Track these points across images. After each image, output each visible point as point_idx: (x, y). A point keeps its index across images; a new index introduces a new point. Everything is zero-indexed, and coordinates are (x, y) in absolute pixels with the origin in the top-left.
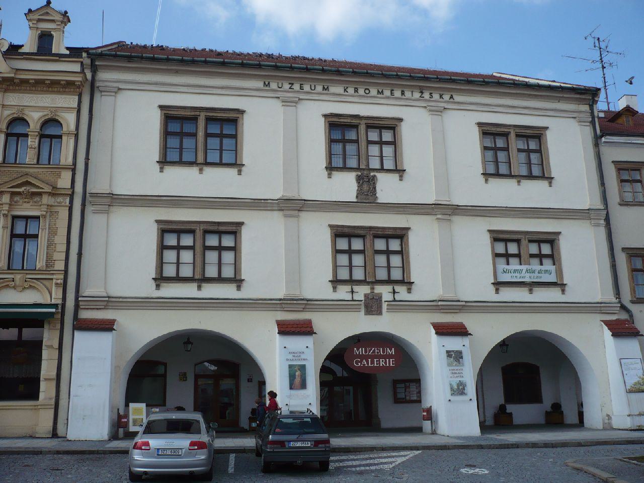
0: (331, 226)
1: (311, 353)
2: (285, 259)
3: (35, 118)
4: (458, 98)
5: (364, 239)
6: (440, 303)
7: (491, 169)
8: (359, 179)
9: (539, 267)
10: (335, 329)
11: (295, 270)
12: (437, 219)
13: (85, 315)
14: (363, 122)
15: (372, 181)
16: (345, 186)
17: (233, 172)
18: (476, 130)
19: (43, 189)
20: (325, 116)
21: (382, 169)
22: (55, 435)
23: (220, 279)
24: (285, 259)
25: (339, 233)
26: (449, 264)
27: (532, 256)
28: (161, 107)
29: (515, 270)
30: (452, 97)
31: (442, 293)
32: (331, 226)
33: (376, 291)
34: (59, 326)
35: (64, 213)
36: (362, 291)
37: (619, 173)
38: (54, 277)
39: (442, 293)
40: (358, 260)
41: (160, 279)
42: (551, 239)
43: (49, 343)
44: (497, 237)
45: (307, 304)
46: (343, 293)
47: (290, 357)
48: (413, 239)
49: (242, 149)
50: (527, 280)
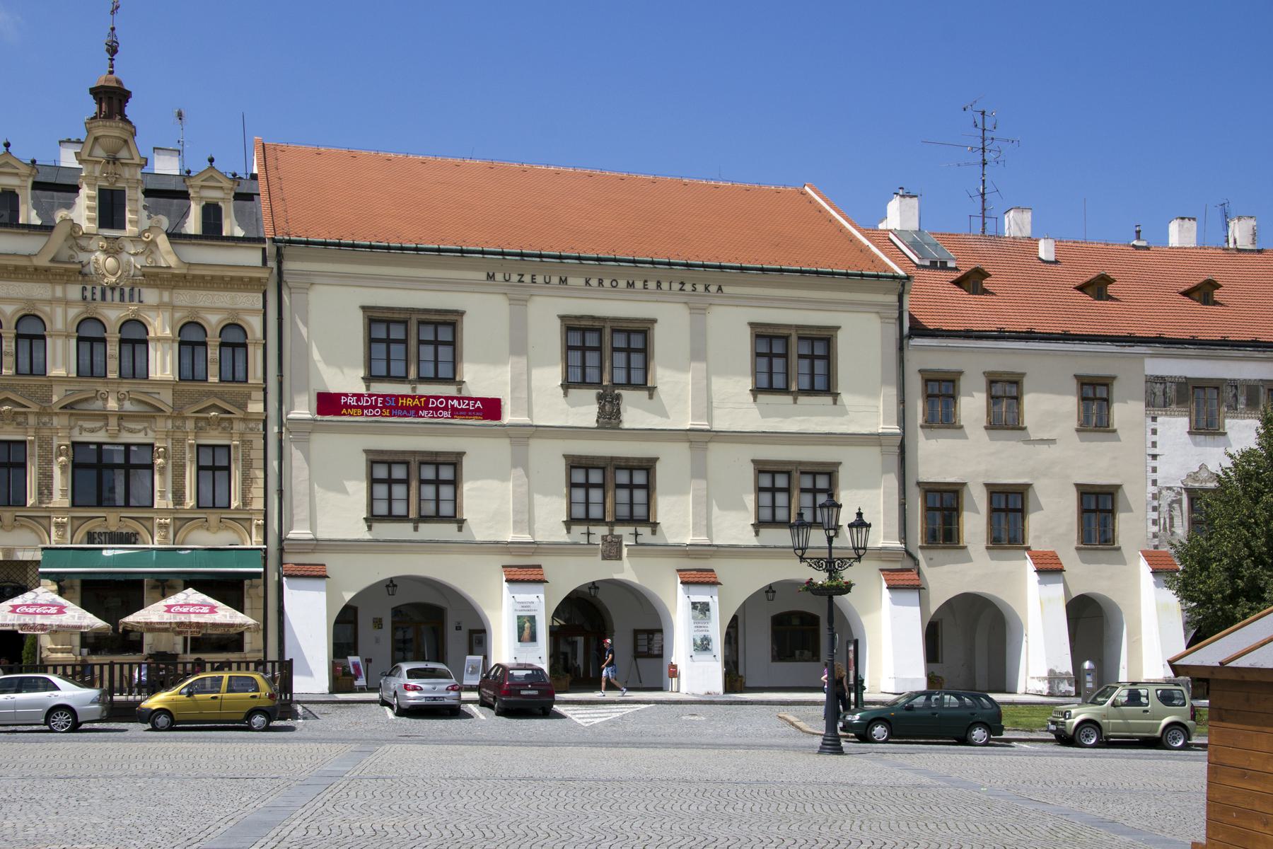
8: (600, 398)
21: (629, 385)
23: (437, 518)
30: (720, 289)
36: (600, 531)
45: (535, 547)
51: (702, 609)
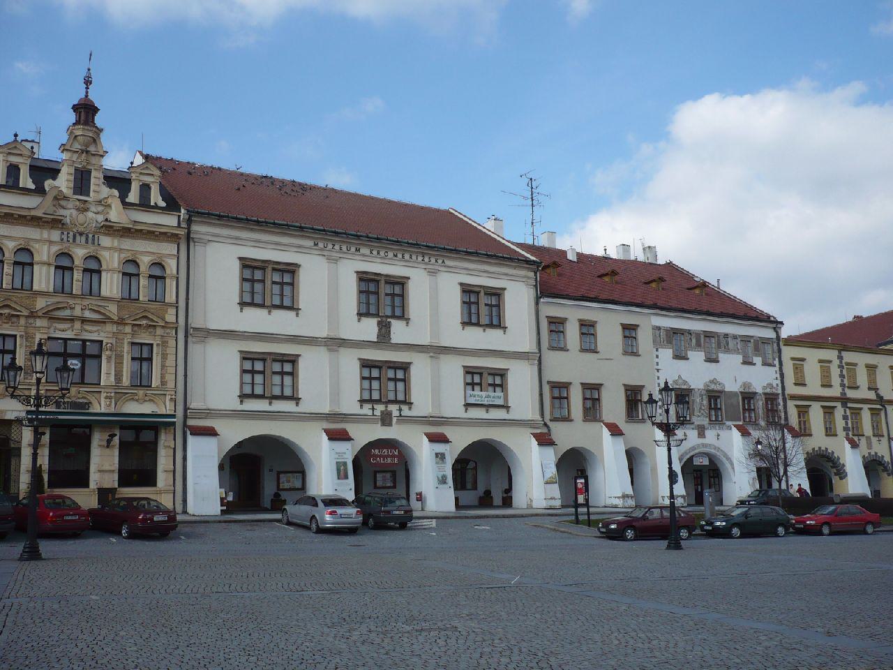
0: (359, 359)
1: (347, 452)
2: (328, 382)
3: (145, 261)
4: (448, 262)
5: (293, 365)
6: (430, 419)
7: (466, 320)
8: (379, 323)
9: (492, 394)
10: (364, 434)
11: (336, 394)
12: (431, 357)
13: (191, 422)
14: (383, 279)
15: (388, 326)
16: (369, 329)
17: (292, 314)
18: (458, 288)
19: (21, 312)
20: (357, 272)
21: (394, 316)
22: (423, 510)
23: (282, 397)
24: (328, 382)
25: (366, 364)
26: (436, 390)
27: (490, 385)
28: (240, 259)
29: (479, 396)
30: (443, 262)
31: (430, 411)
32: (359, 359)
33: (389, 409)
34: (173, 431)
35: (172, 343)
36: (380, 408)
37: (624, 331)
38: (168, 393)
39: (430, 411)
40: (375, 384)
41: (243, 397)
42: (502, 374)
43: (166, 444)
44: (469, 371)
45: (344, 417)
46: (367, 410)
47: (337, 456)
48: (413, 370)
49: (298, 297)
50: (486, 403)
51: (440, 457)
